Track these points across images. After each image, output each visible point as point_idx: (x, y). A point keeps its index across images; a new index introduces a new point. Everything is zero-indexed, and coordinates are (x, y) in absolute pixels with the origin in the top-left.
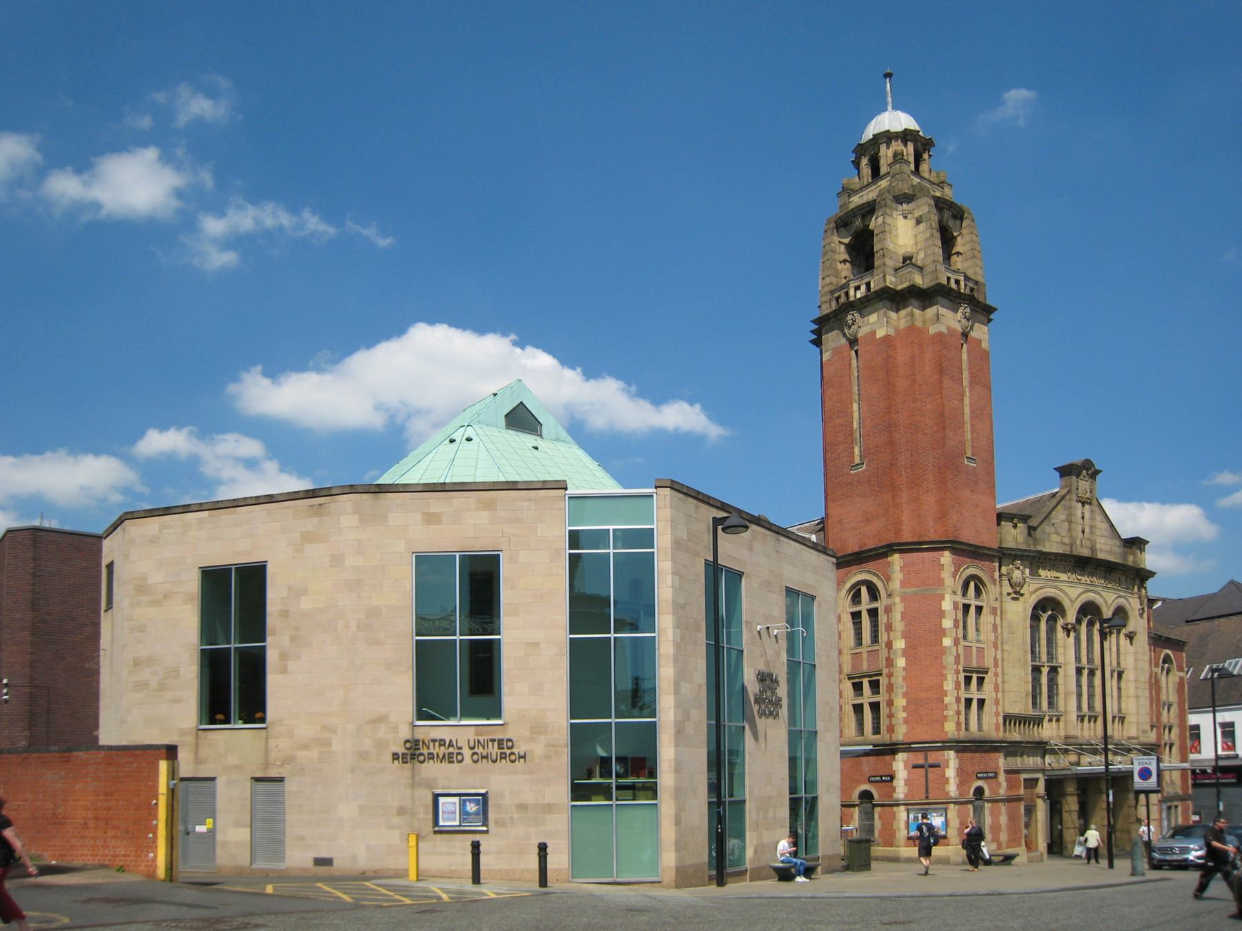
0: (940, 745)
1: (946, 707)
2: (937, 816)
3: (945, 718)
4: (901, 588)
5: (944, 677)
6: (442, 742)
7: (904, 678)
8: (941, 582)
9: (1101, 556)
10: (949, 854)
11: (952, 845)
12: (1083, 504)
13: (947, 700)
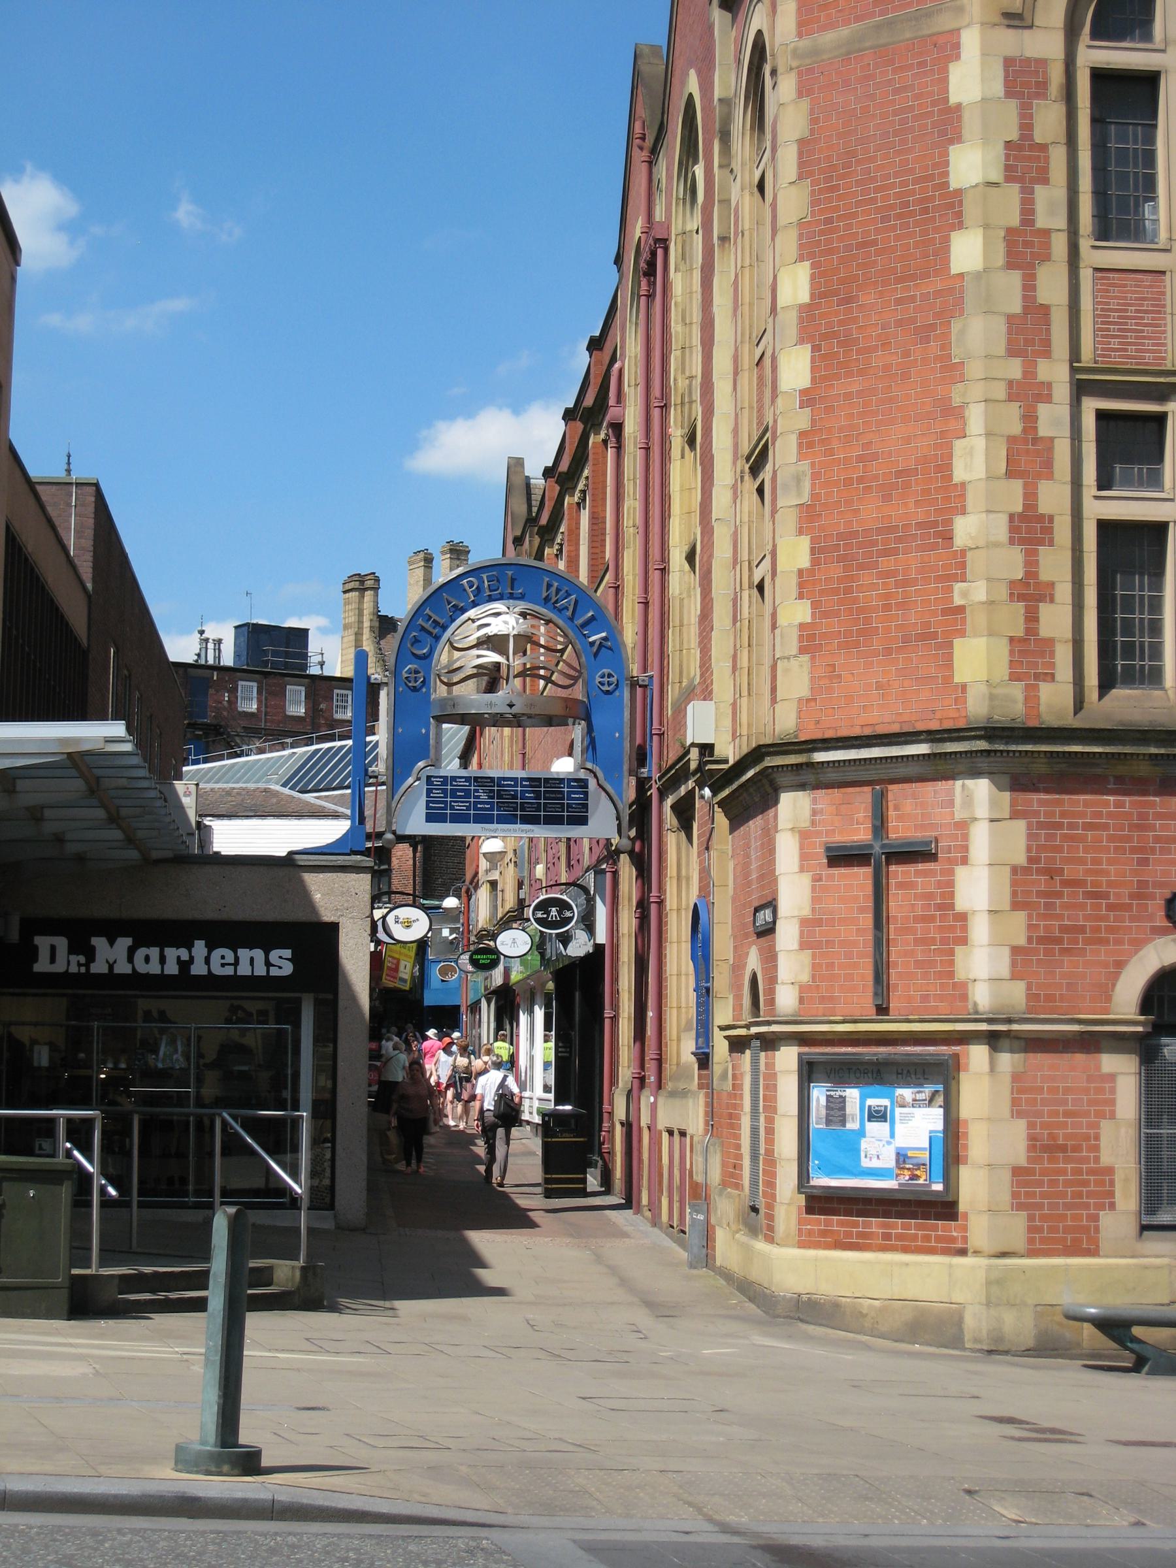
0: (922, 749)
1: (958, 568)
2: (916, 1103)
4: (800, 35)
7: (806, 441)
10: (958, 1297)
11: (976, 1253)
13: (965, 529)
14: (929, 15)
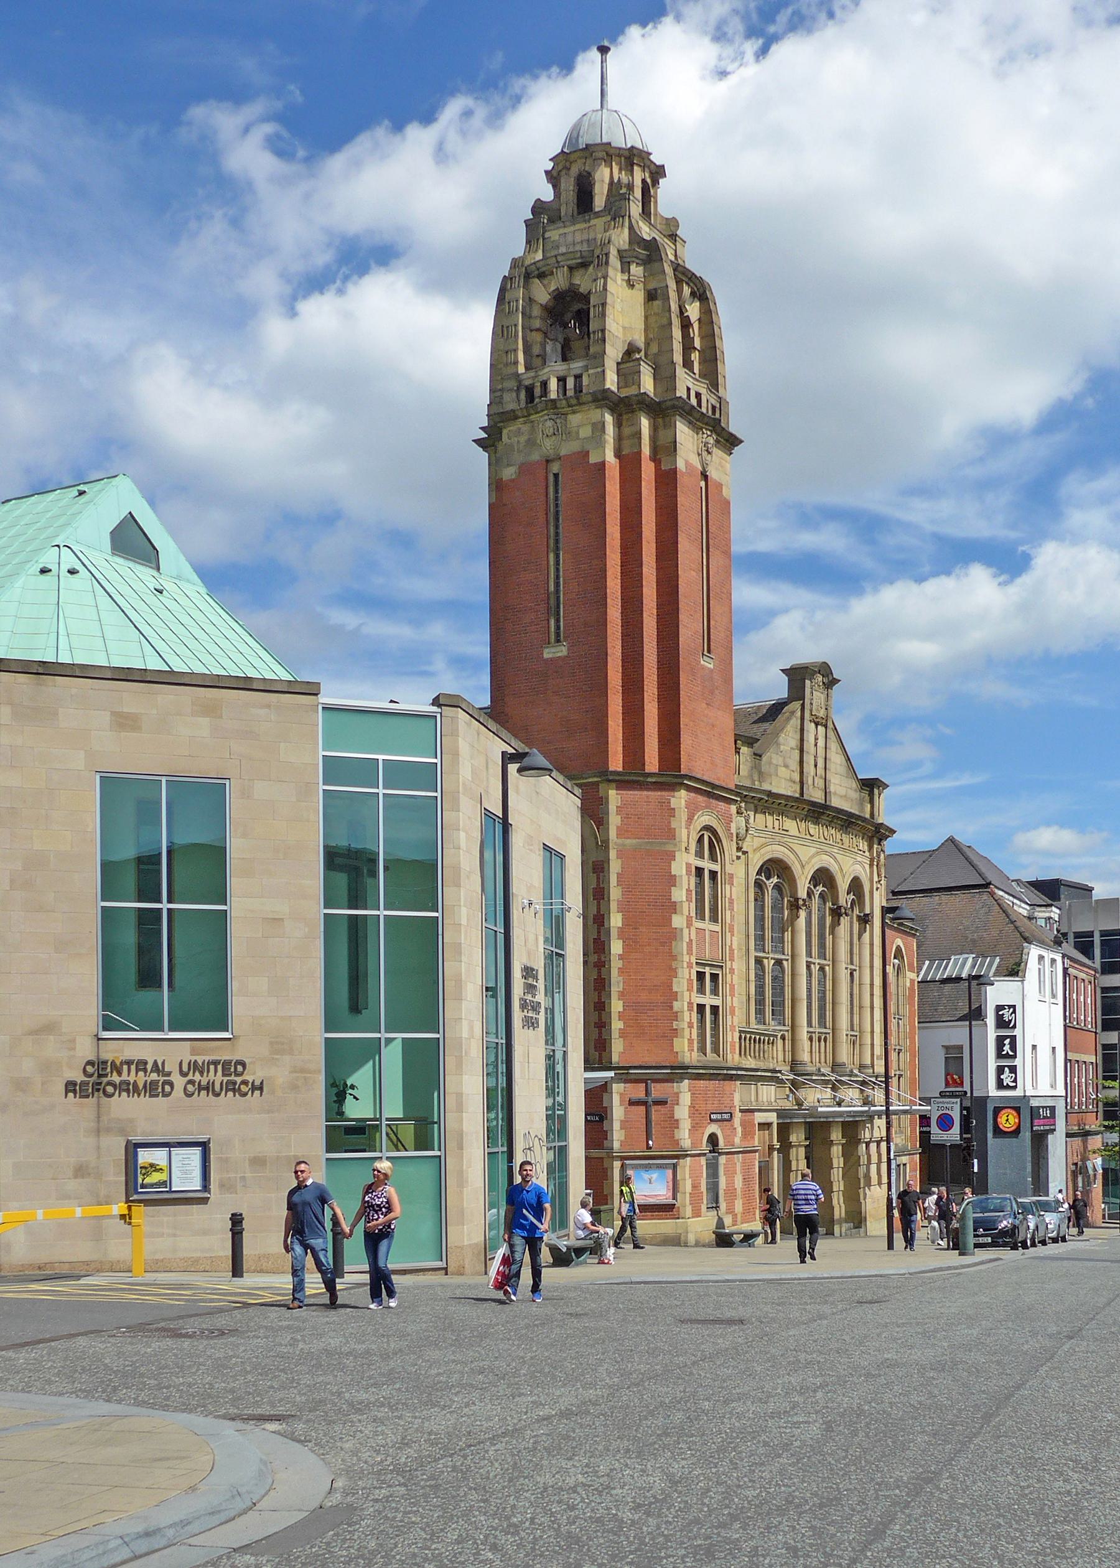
3: (675, 1032)
5: (673, 972)
6: (141, 1065)
8: (671, 835)
9: (835, 802)
12: (817, 724)
13: (676, 1005)
14: (665, 844)
